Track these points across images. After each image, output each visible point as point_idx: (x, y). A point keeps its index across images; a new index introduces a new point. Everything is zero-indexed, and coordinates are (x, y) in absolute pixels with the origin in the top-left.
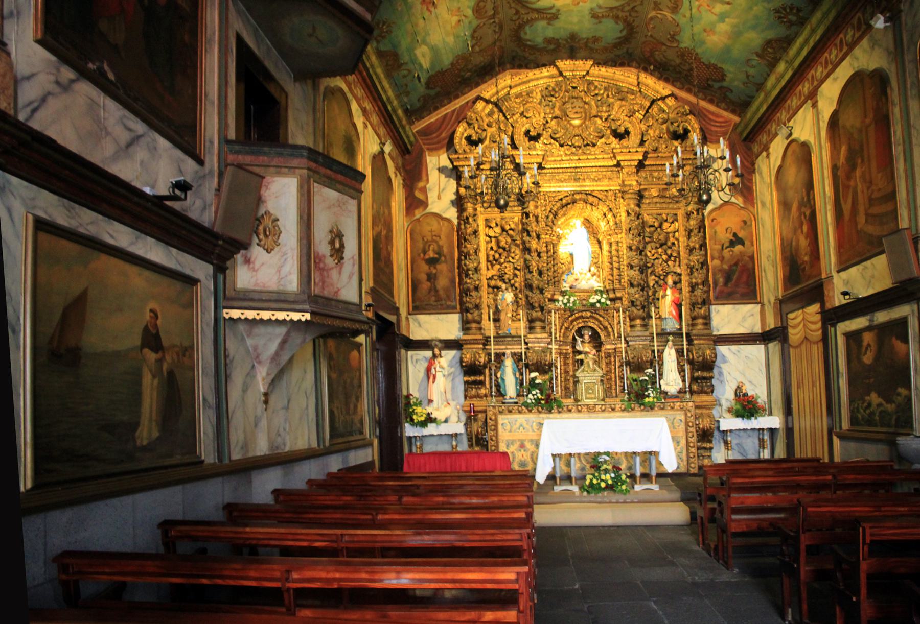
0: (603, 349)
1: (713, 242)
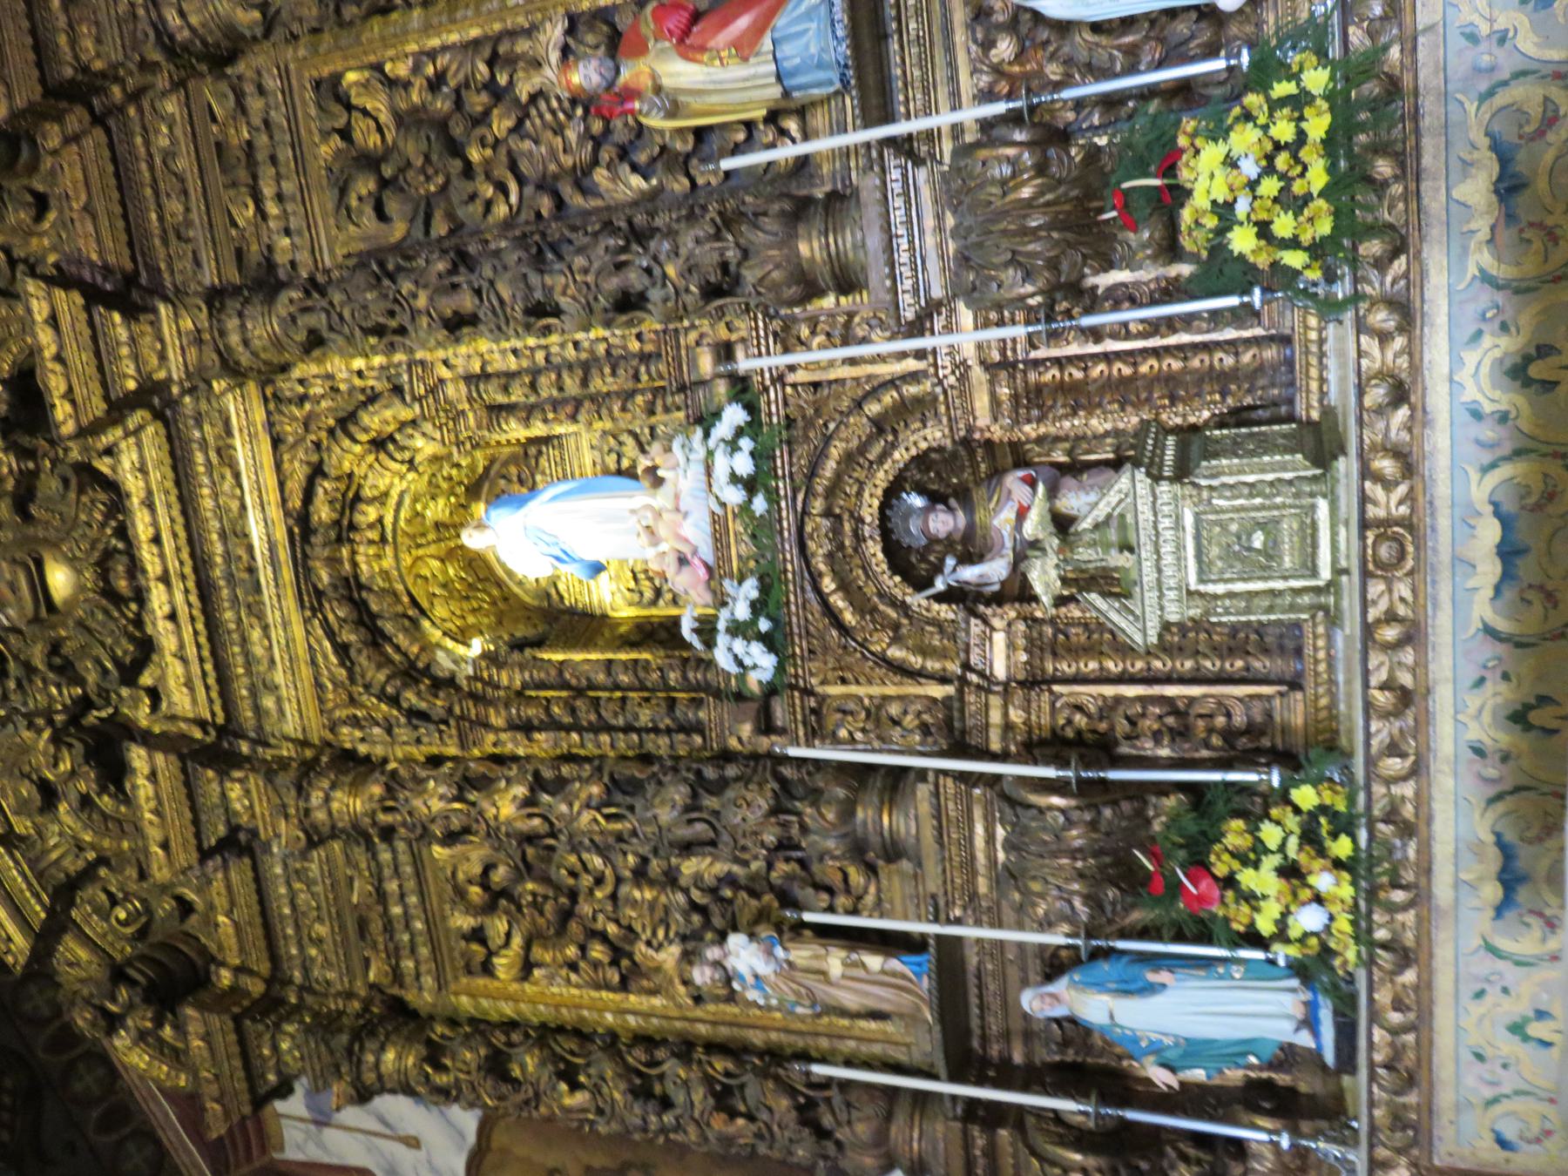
0: (997, 433)
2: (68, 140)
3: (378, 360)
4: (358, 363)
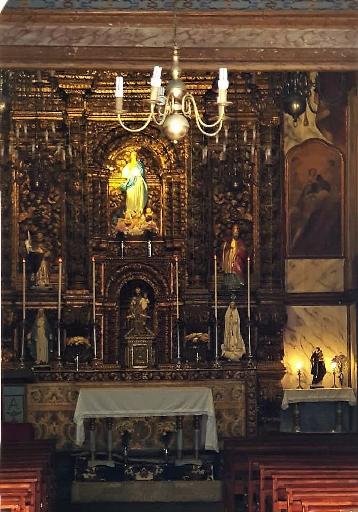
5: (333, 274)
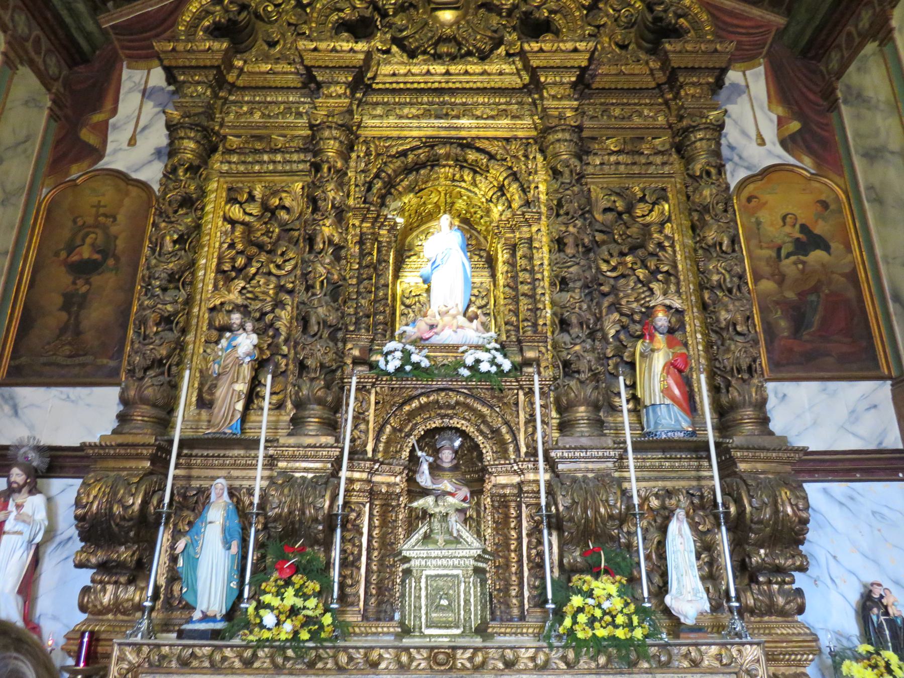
0: (488, 486)
1: (754, 242)
2: (651, 70)
3: (543, 197)
4: (542, 188)
5: (873, 411)
